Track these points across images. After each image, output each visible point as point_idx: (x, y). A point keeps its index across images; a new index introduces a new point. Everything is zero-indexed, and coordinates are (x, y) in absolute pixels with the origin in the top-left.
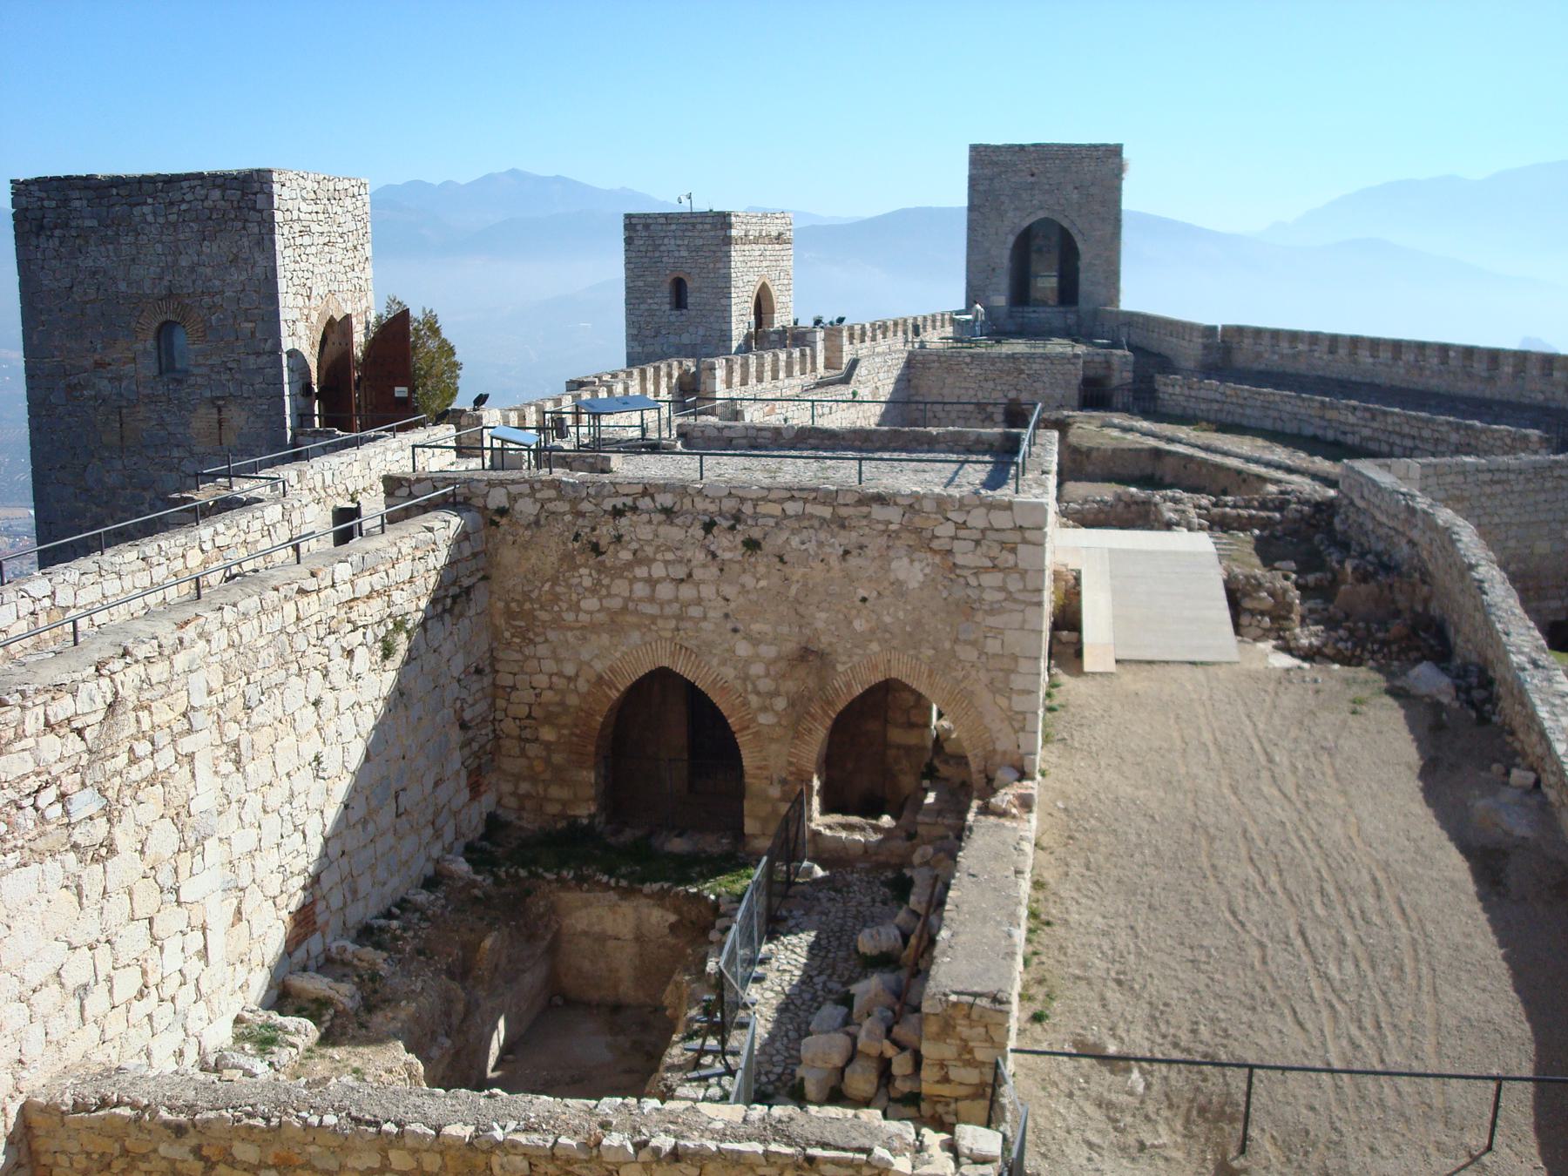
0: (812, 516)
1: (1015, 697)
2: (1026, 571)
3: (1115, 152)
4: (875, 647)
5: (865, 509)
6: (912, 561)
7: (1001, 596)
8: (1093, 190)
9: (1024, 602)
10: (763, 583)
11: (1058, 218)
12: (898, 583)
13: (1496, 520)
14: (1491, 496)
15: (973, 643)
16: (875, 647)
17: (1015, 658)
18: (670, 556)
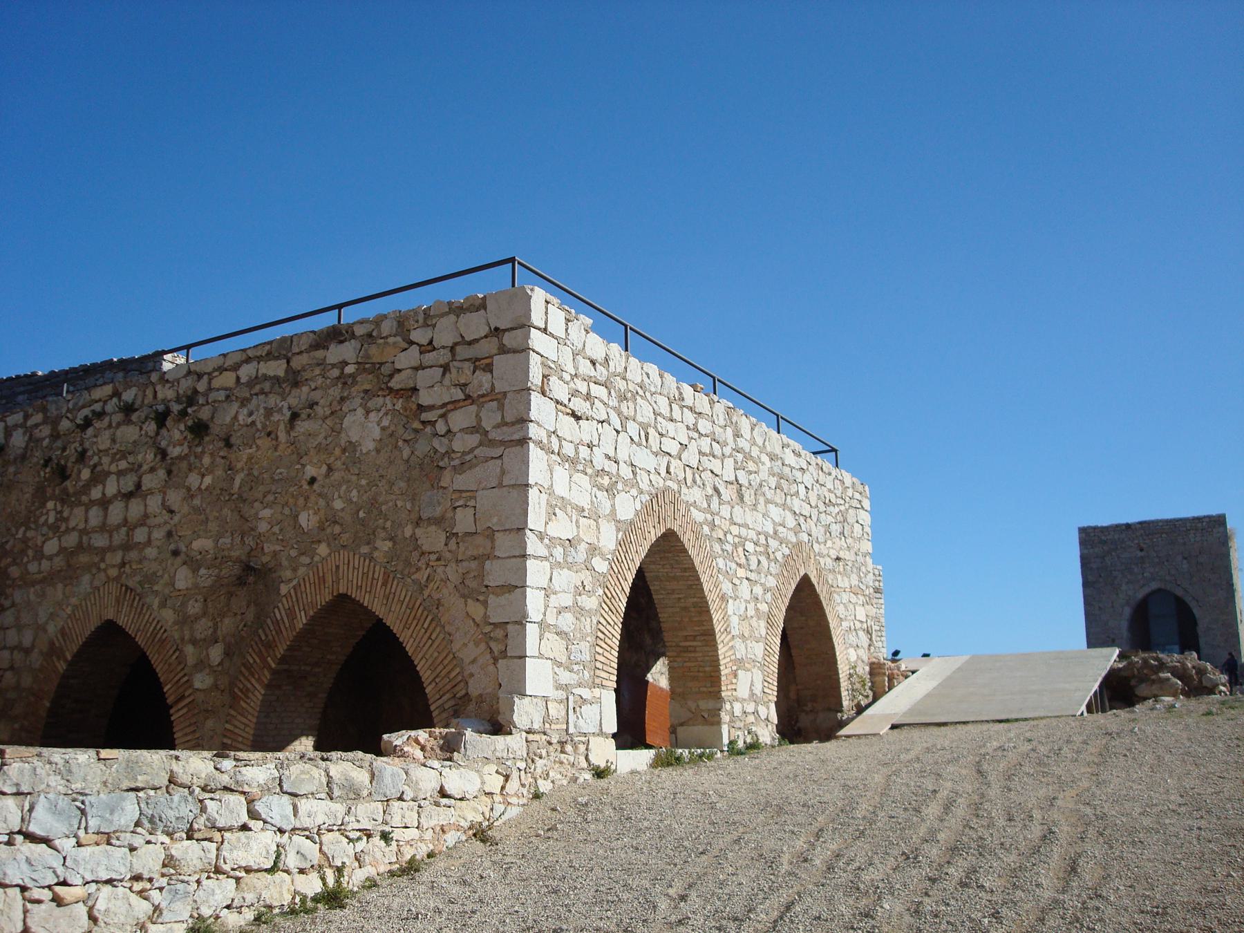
0: (266, 378)
1: (492, 599)
2: (505, 394)
3: (1220, 521)
4: (323, 550)
5: (320, 354)
6: (368, 412)
7: (474, 440)
9: (502, 443)
10: (208, 480)
12: (352, 447)
15: (438, 521)
16: (323, 550)
17: (491, 534)
18: (123, 465)
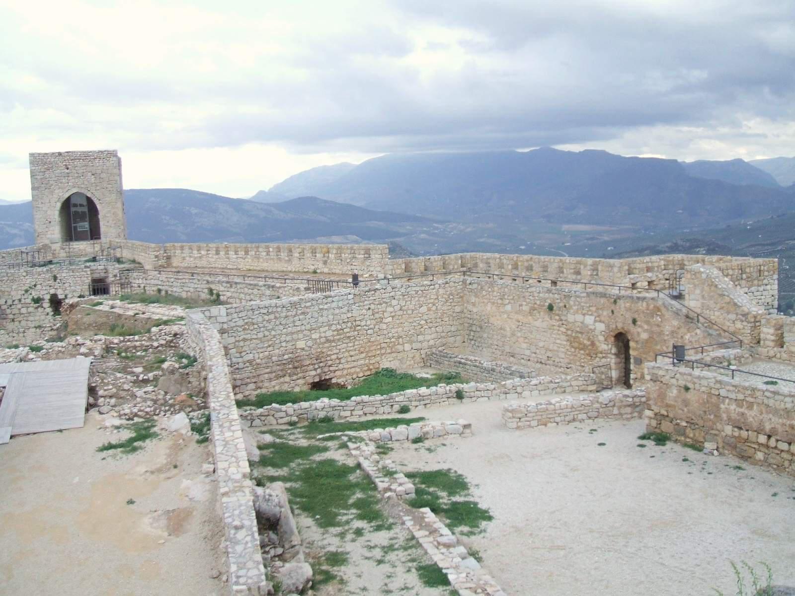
8: (104, 175)
11: (82, 191)
13: (273, 333)
14: (269, 321)
